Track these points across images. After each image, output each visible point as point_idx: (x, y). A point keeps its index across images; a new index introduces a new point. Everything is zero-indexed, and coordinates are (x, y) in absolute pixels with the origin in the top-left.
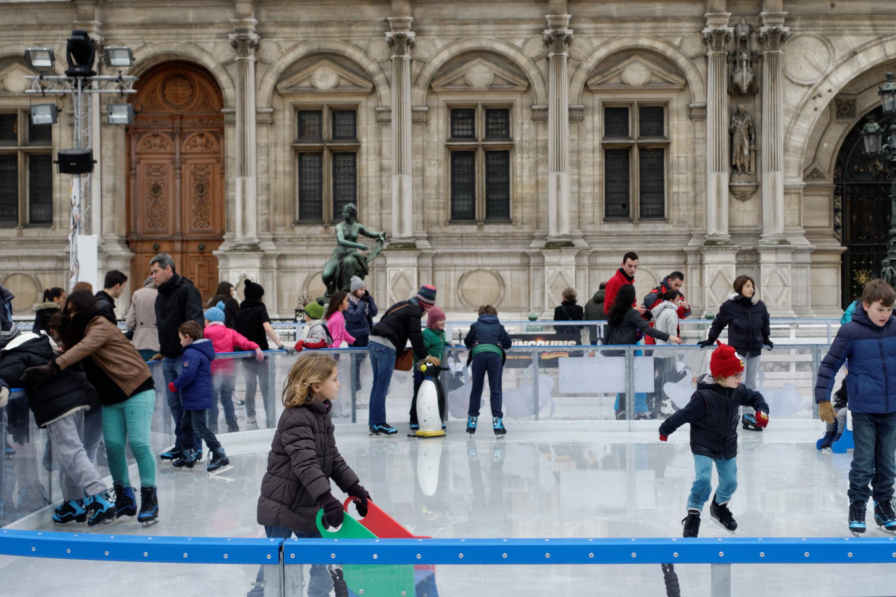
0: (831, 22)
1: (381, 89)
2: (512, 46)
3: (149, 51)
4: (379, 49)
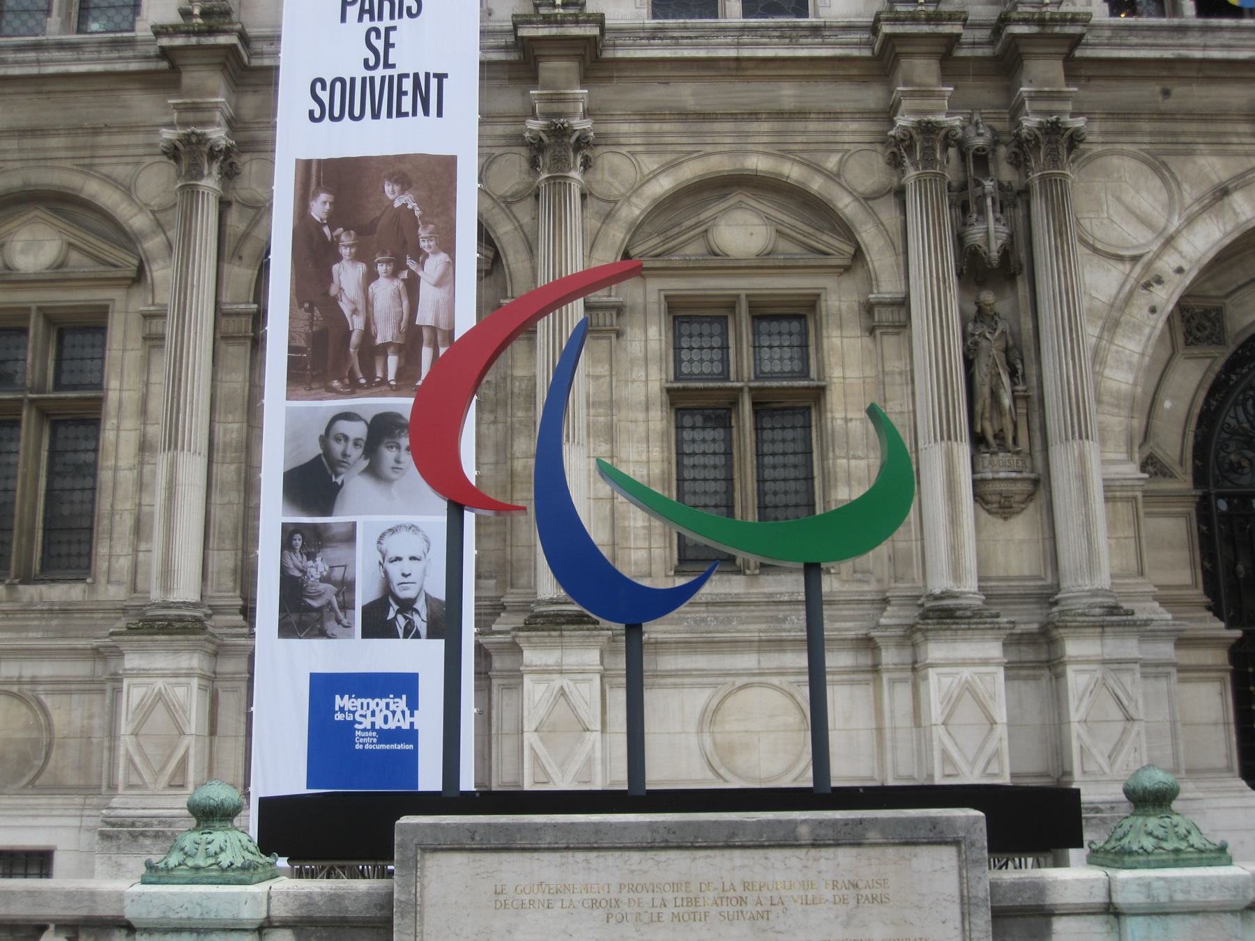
0: (1166, 126)
1: (154, 267)
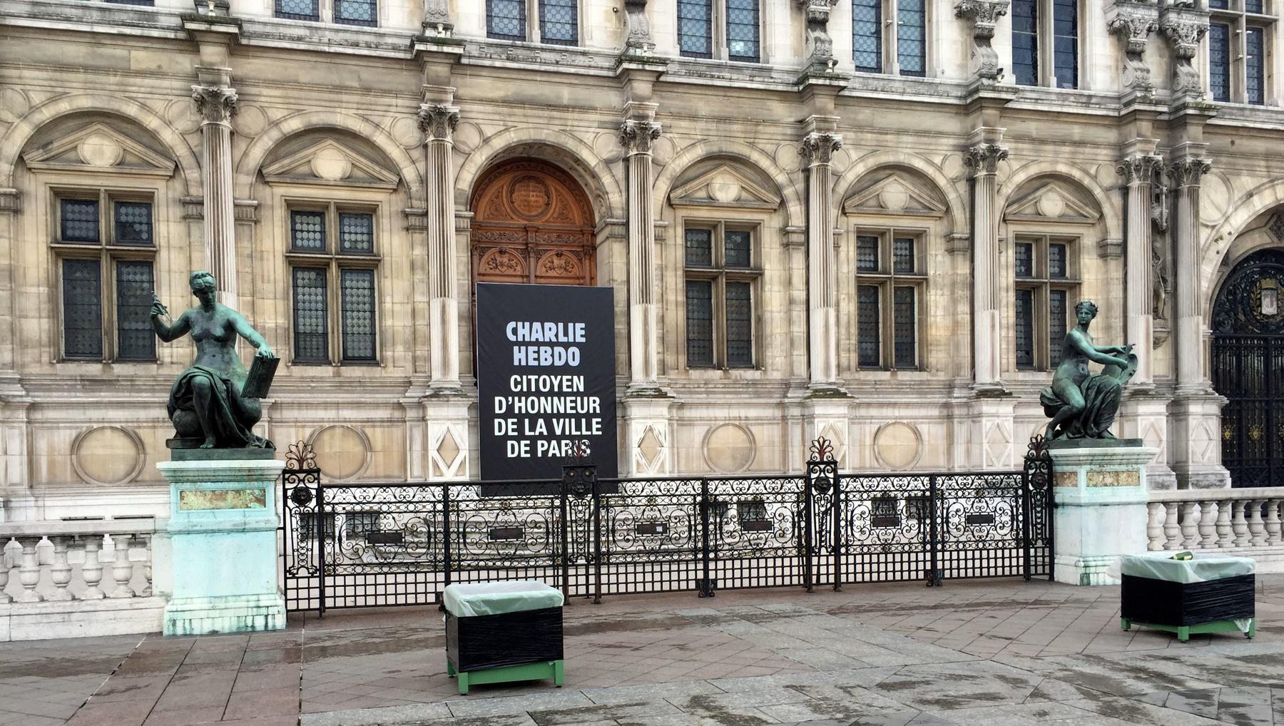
1: (790, 205)
2: (932, 163)
3: (512, 137)
4: (789, 156)
